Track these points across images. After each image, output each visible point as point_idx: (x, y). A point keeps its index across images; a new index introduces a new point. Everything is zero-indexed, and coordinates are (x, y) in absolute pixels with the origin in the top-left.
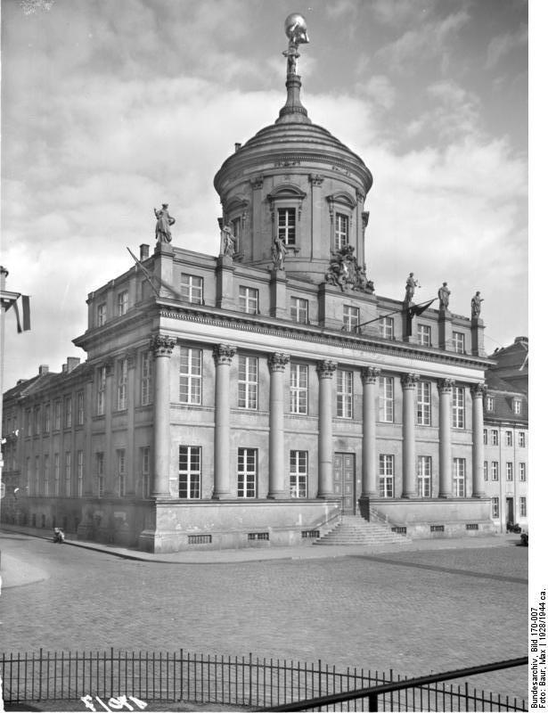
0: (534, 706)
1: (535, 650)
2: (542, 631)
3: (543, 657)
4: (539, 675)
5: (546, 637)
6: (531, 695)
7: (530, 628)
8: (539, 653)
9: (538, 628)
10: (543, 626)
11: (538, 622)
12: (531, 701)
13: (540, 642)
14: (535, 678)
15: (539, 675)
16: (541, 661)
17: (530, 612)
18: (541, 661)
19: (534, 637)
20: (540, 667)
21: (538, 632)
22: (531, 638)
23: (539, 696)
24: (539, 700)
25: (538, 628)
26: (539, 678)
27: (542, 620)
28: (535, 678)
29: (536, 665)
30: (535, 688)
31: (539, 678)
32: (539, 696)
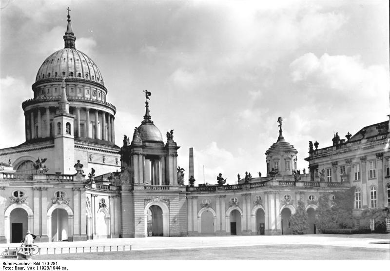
0: (4, 263)
1: (35, 264)
2: (45, 268)
3: (31, 268)
4: (21, 266)
7: (47, 261)
8: (33, 266)
9: (46, 265)
13: (39, 266)
14: (19, 264)
15: (21, 266)
16: (29, 267)
18: (29, 267)
20: (25, 267)
21: (44, 266)
23: (9, 266)
24: (7, 266)
25: (46, 265)
26: (19, 266)
27: (51, 268)
28: (19, 264)
29: (26, 264)
30: (14, 264)
31: (19, 266)
32: (9, 266)
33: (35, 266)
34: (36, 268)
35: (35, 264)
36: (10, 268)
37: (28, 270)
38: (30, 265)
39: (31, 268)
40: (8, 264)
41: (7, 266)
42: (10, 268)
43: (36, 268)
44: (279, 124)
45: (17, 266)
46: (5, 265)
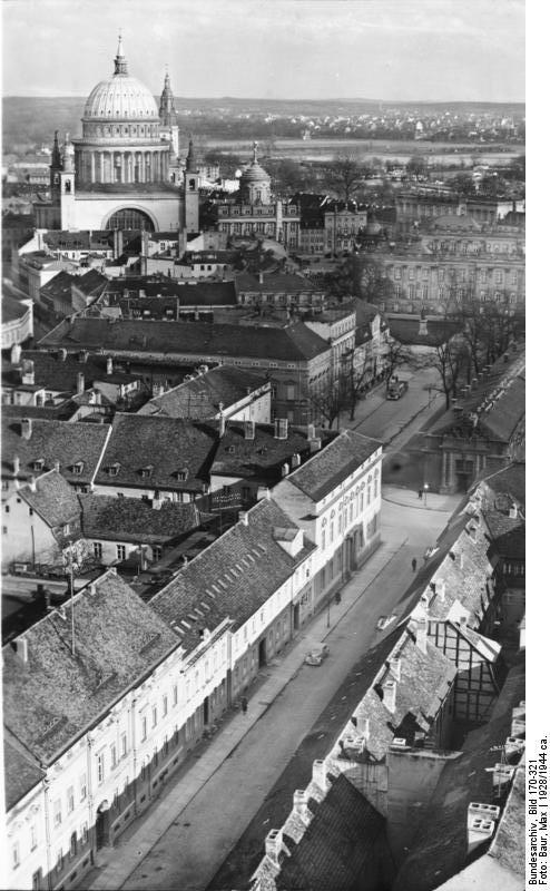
0: (533, 882)
2: (543, 789)
3: (543, 821)
4: (539, 844)
5: (548, 796)
8: (539, 817)
9: (537, 785)
10: (542, 782)
11: (537, 778)
13: (539, 802)
15: (539, 844)
16: (541, 826)
18: (541, 826)
21: (537, 790)
23: (539, 869)
24: (539, 875)
25: (537, 785)
27: (543, 775)
28: (534, 848)
29: (535, 831)
30: (534, 860)
32: (539, 869)
38: (537, 823)
41: (539, 875)
44: (300, 672)
45: (538, 852)
46: (537, 879)
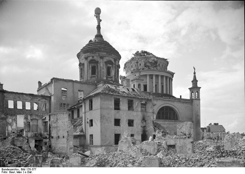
0: (2, 169)
1: (22, 169)
3: (19, 172)
4: (13, 171)
6: (6, 168)
8: (20, 171)
12: (4, 168)
13: (24, 171)
14: (12, 170)
15: (13, 171)
16: (18, 171)
17: (36, 168)
18: (18, 171)
19: (26, 169)
20: (16, 171)
22: (26, 168)
23: (6, 171)
24: (4, 171)
28: (12, 170)
29: (16, 170)
30: (9, 169)
31: (11, 171)
32: (6, 171)
33: (22, 171)
34: (22, 172)
35: (22, 169)
36: (7, 172)
37: (17, 173)
39: (19, 172)
40: (5, 169)
42: (7, 172)
43: (22, 172)
